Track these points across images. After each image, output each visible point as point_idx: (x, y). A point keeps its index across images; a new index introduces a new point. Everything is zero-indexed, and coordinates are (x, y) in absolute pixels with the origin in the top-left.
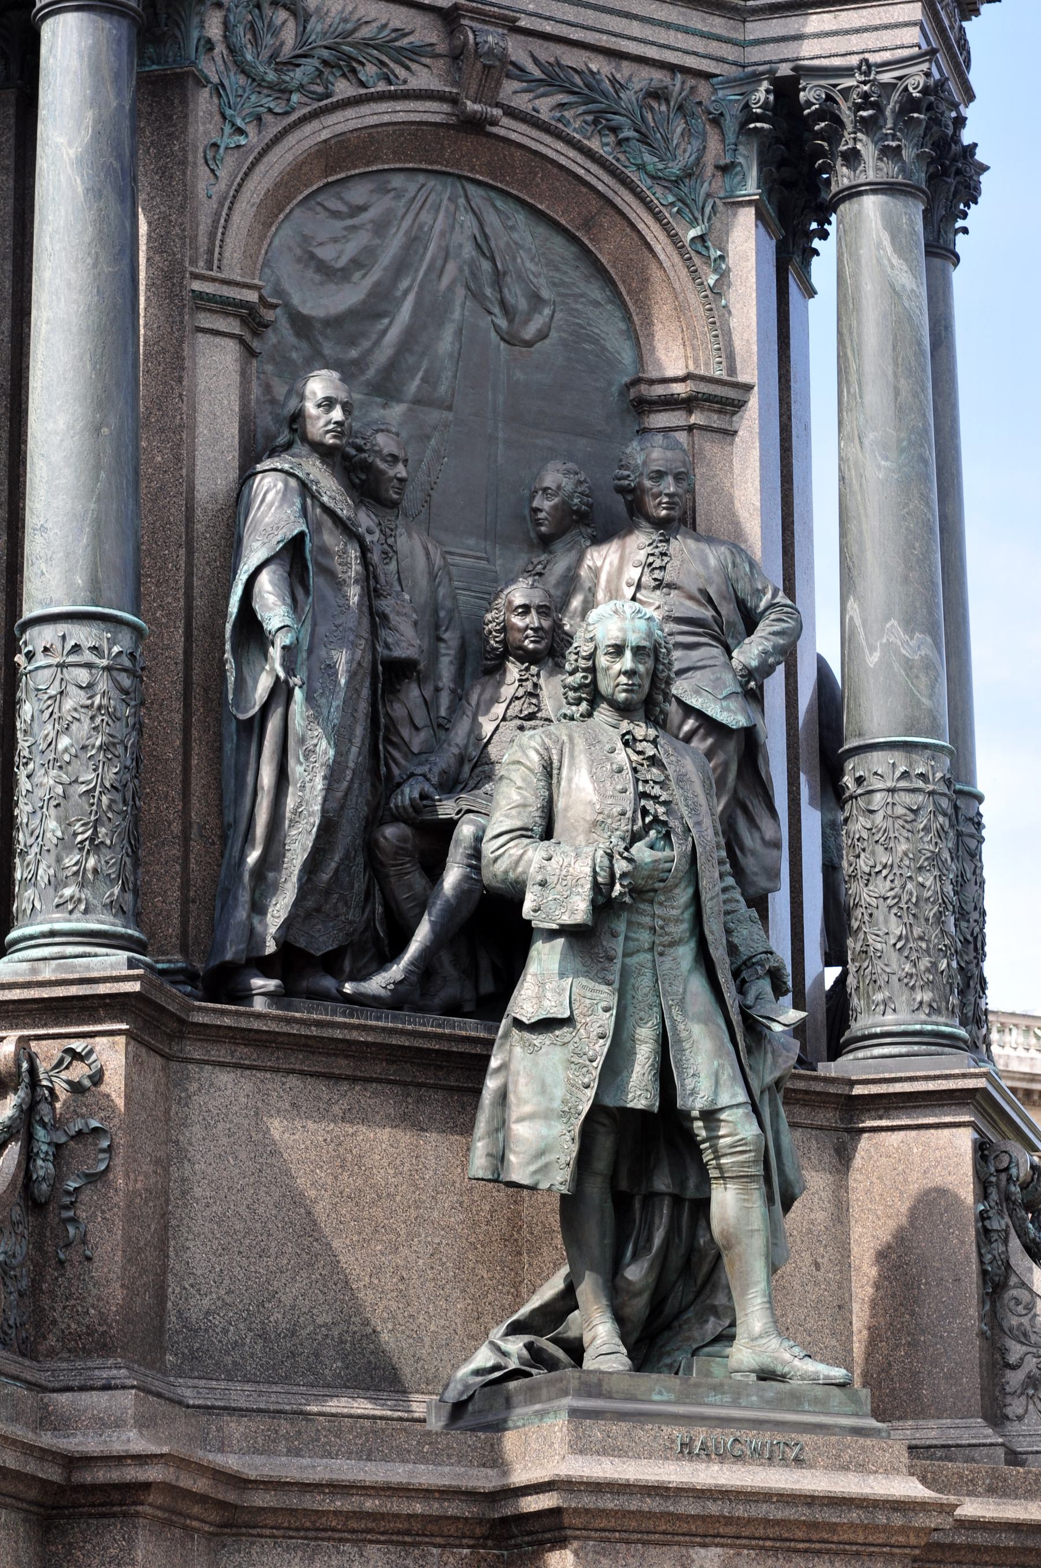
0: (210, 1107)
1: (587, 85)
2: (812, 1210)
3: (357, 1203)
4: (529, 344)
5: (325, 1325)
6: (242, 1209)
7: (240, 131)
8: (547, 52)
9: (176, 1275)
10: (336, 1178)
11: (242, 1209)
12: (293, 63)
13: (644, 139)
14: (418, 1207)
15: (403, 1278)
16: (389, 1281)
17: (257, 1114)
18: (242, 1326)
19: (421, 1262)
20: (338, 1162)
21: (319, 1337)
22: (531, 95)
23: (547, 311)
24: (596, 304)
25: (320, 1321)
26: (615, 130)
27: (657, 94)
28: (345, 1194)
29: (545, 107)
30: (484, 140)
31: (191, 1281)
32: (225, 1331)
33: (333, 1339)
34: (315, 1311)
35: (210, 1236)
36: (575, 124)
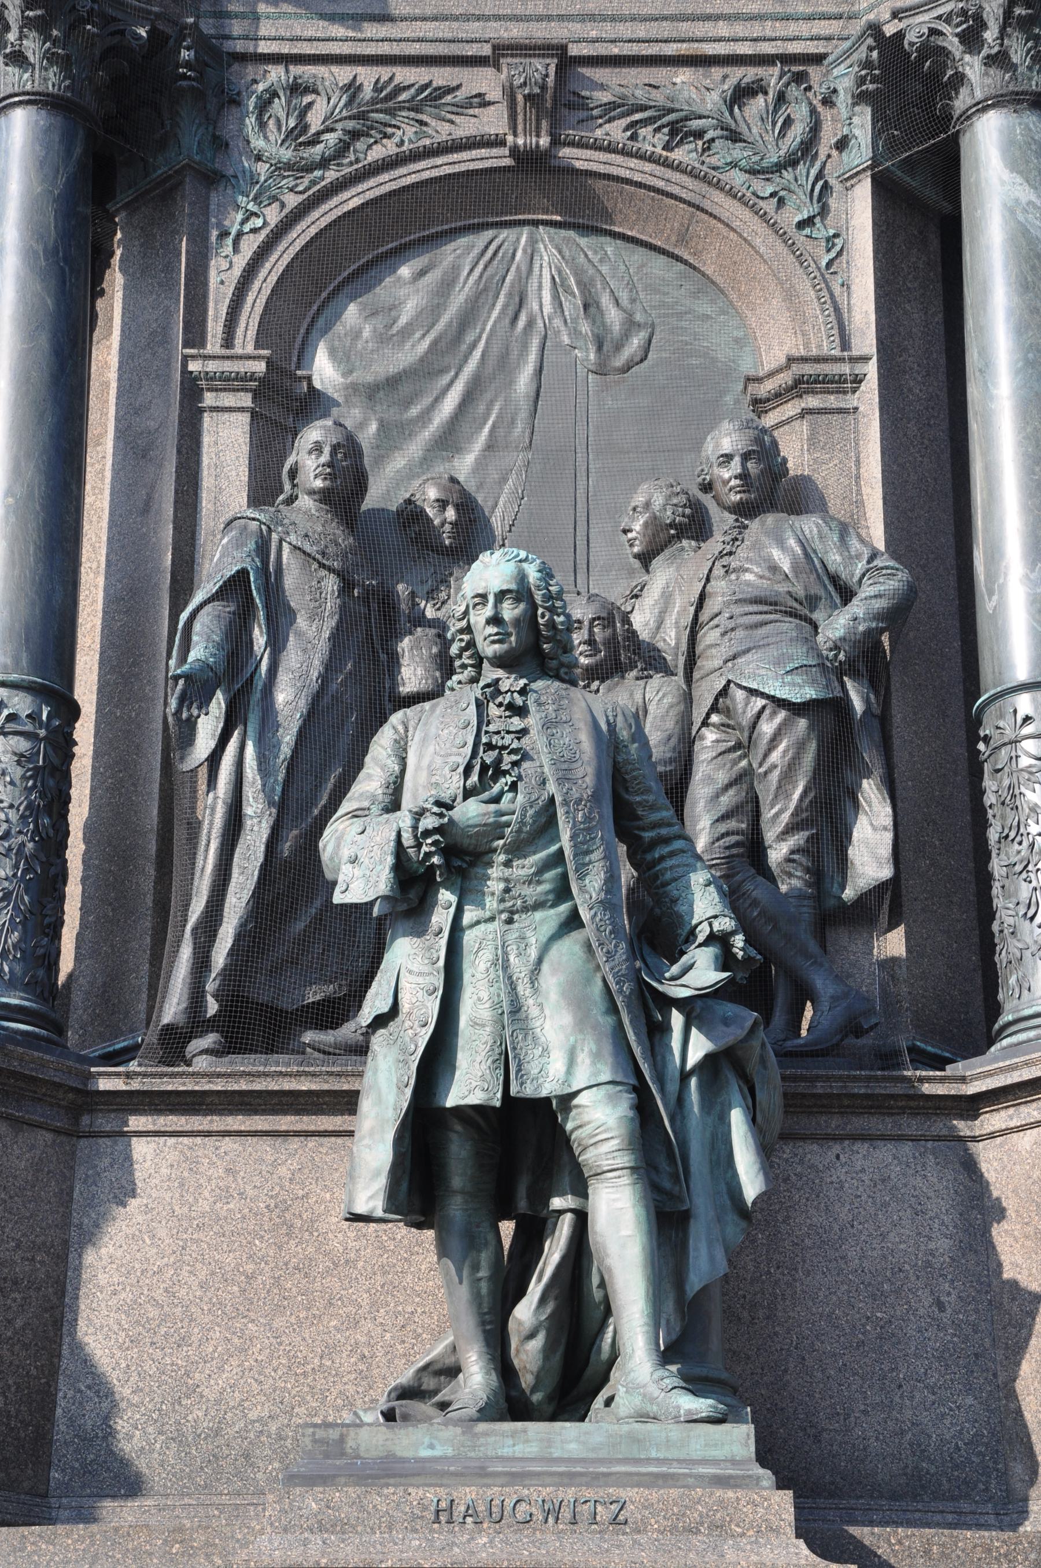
2: (930, 1238)
3: (306, 1275)
5: (260, 1420)
6: (159, 1294)
9: (69, 1377)
10: (280, 1248)
11: (159, 1294)
12: (314, 141)
14: (385, 1273)
16: (346, 1361)
17: (182, 1185)
18: (150, 1430)
19: (388, 1336)
20: (284, 1230)
23: (643, 335)
25: (253, 1415)
26: (699, 134)
31: (89, 1381)
33: (269, 1436)
35: (116, 1327)
36: (652, 141)
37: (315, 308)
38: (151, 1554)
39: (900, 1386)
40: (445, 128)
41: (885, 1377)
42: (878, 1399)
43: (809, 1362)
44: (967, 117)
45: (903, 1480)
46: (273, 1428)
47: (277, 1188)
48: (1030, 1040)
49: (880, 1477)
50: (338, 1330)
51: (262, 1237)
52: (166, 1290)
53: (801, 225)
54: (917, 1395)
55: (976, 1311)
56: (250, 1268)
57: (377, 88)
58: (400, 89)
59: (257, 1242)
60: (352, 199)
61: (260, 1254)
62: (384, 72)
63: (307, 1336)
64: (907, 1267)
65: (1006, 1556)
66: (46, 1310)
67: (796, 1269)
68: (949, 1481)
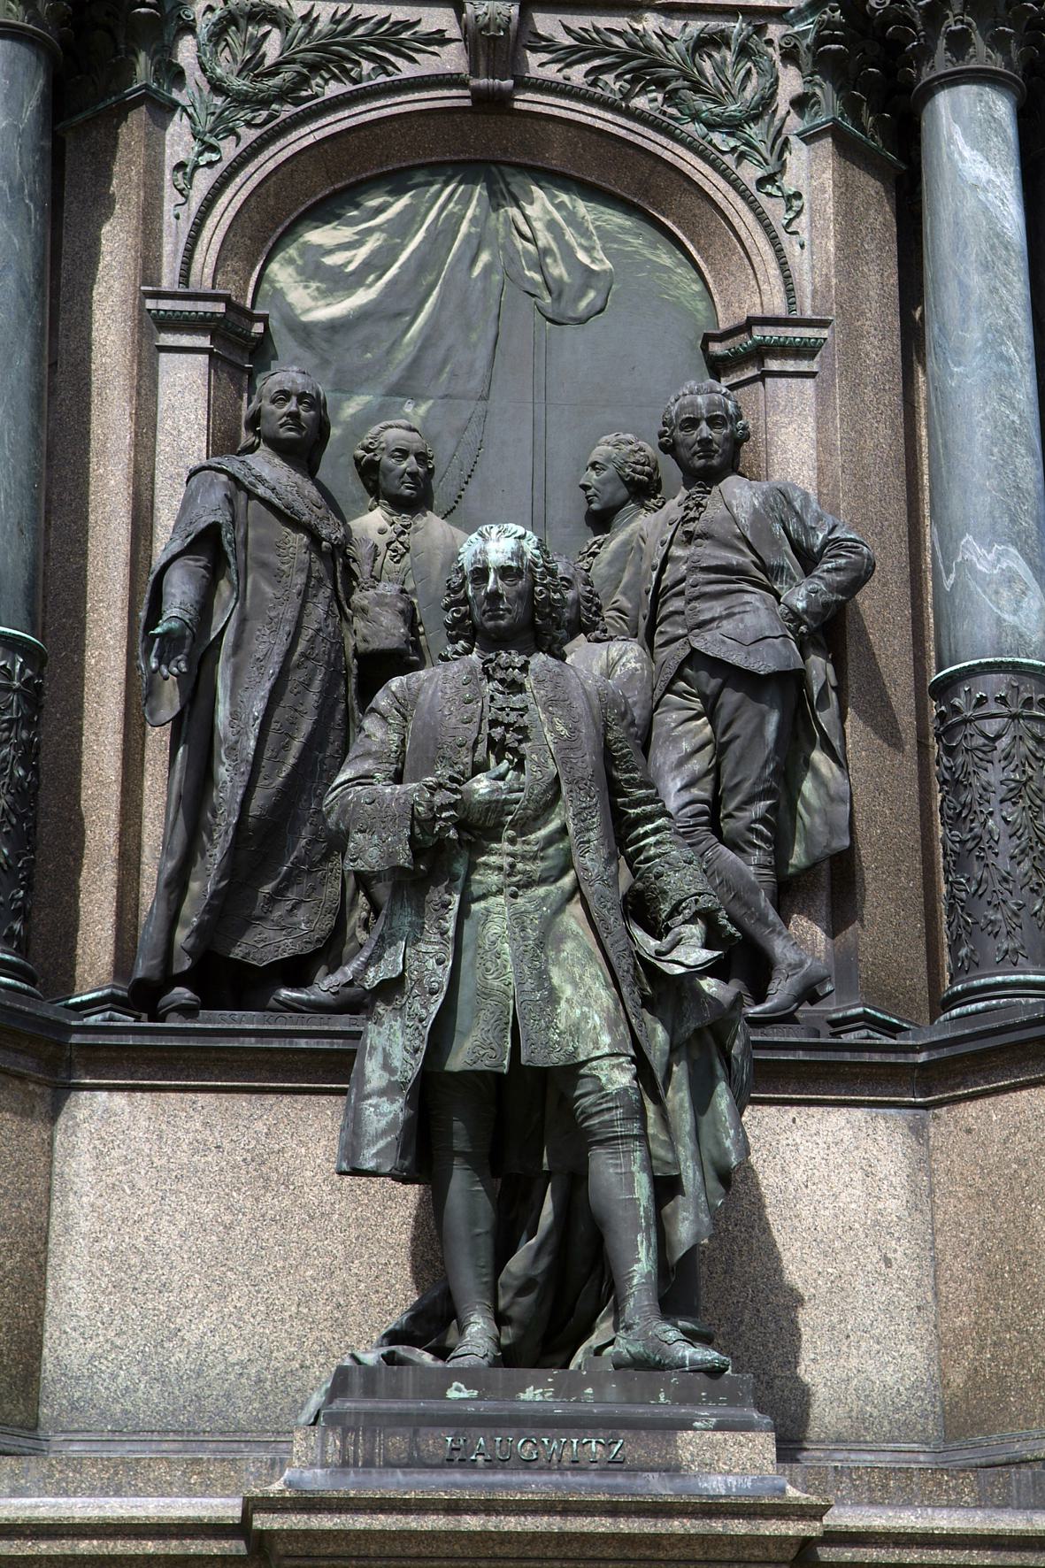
0: (103, 1134)
1: (630, 44)
2: (879, 1199)
6: (140, 1242)
7: (213, 149)
13: (696, 87)
14: (360, 1226)
15: (339, 1305)
18: (134, 1370)
19: (362, 1285)
21: (232, 1377)
22: (560, 66)
25: (232, 1359)
28: (268, 1217)
29: (577, 75)
30: (508, 118)
32: (114, 1377)
34: (227, 1348)
36: (612, 84)
37: (270, 244)
38: (171, 1484)
39: (848, 1337)
40: (400, 62)
41: (833, 1328)
42: (827, 1348)
43: (764, 1314)
44: (929, 91)
45: (848, 1423)
46: (253, 1371)
47: (253, 1143)
48: (977, 1012)
49: (827, 1420)
50: (314, 1280)
51: (239, 1189)
52: (146, 1239)
54: (863, 1344)
55: (920, 1267)
56: (227, 1218)
57: (335, 21)
58: (358, 22)
59: (234, 1194)
60: (306, 136)
61: (237, 1206)
63: (284, 1284)
64: (857, 1225)
65: (954, 1488)
66: (32, 1255)
67: (753, 1228)
68: (890, 1423)
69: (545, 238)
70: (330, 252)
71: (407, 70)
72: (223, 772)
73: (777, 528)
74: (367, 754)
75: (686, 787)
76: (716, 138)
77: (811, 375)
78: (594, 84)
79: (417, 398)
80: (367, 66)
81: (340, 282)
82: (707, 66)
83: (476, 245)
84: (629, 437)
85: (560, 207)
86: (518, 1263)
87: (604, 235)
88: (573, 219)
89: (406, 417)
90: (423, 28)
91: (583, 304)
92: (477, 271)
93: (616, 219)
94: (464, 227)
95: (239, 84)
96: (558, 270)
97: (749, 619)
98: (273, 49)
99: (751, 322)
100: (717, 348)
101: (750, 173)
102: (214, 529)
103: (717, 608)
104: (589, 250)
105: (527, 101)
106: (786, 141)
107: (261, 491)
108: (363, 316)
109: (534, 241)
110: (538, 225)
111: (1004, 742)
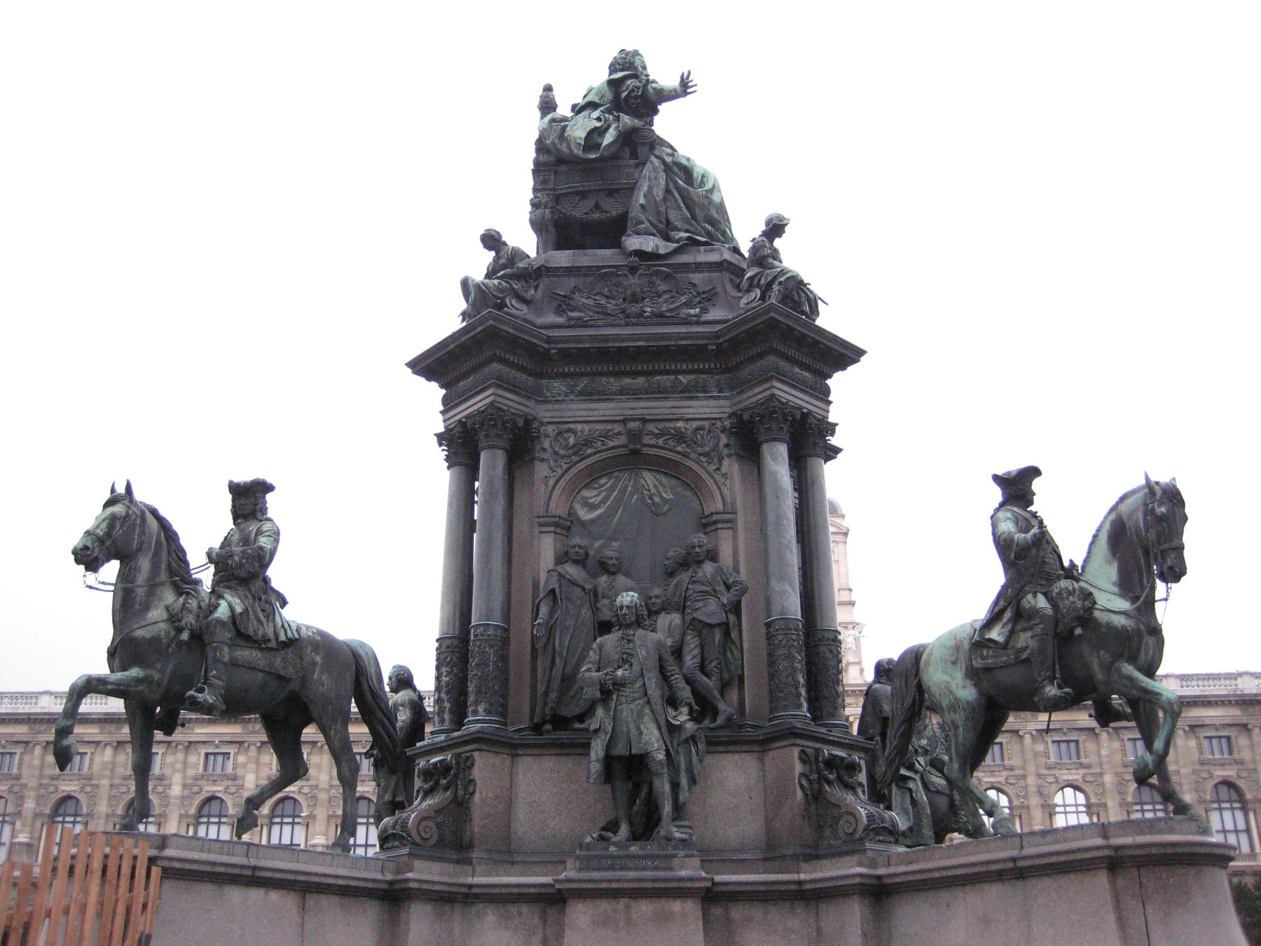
4: (664, 514)
8: (661, 425)
24: (689, 497)
27: (698, 429)
29: (661, 442)
36: (671, 443)
40: (609, 442)
53: (715, 470)
57: (589, 431)
60: (582, 465)
62: (592, 426)
69: (653, 490)
70: (591, 498)
71: (611, 444)
72: (557, 661)
73: (719, 578)
74: (589, 663)
75: (691, 659)
76: (701, 458)
77: (731, 528)
78: (665, 444)
79: (616, 540)
80: (599, 443)
81: (593, 507)
82: (699, 436)
83: (632, 494)
84: (678, 549)
85: (658, 480)
86: (635, 808)
87: (671, 488)
88: (661, 483)
89: (613, 547)
90: (616, 431)
91: (665, 509)
92: (633, 501)
93: (674, 482)
94: (629, 488)
95: (562, 452)
96: (657, 499)
97: (710, 607)
98: (572, 441)
99: (712, 514)
100: (703, 521)
101: (712, 468)
102: (553, 591)
103: (701, 604)
104: (666, 493)
105: (646, 450)
106: (723, 458)
107: (567, 576)
108: (599, 517)
109: (649, 491)
110: (651, 486)
111: (784, 642)
